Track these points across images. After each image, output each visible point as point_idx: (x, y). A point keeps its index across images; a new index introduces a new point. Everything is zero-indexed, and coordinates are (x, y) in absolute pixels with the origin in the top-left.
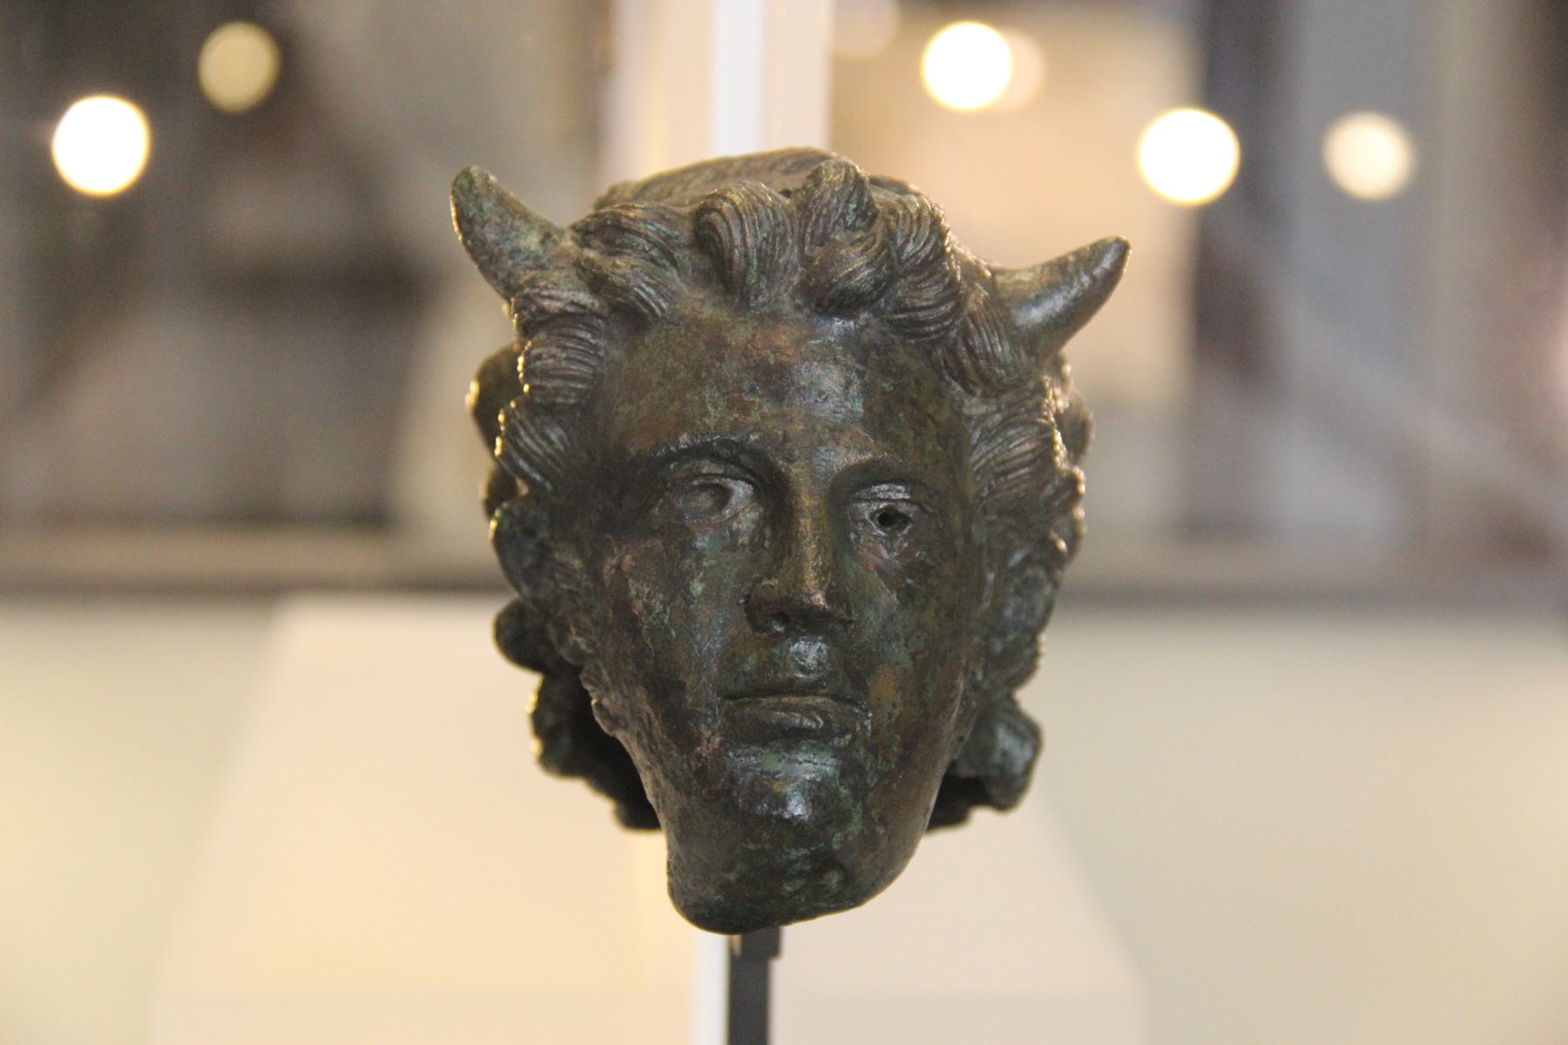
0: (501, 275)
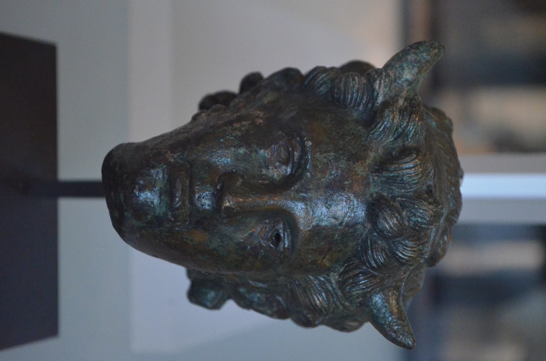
0: (393, 63)
